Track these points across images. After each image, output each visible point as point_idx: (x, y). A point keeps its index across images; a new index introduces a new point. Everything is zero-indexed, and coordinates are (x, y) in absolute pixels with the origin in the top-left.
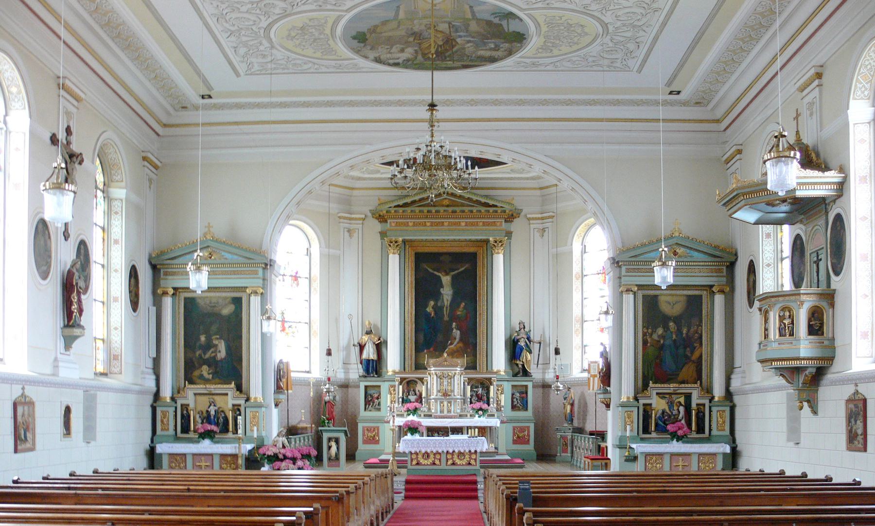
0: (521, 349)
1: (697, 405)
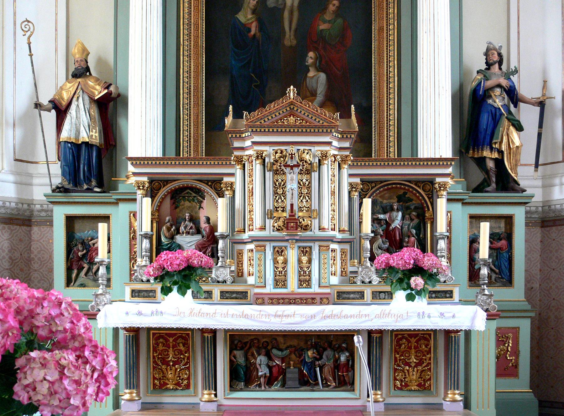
0: (496, 117)
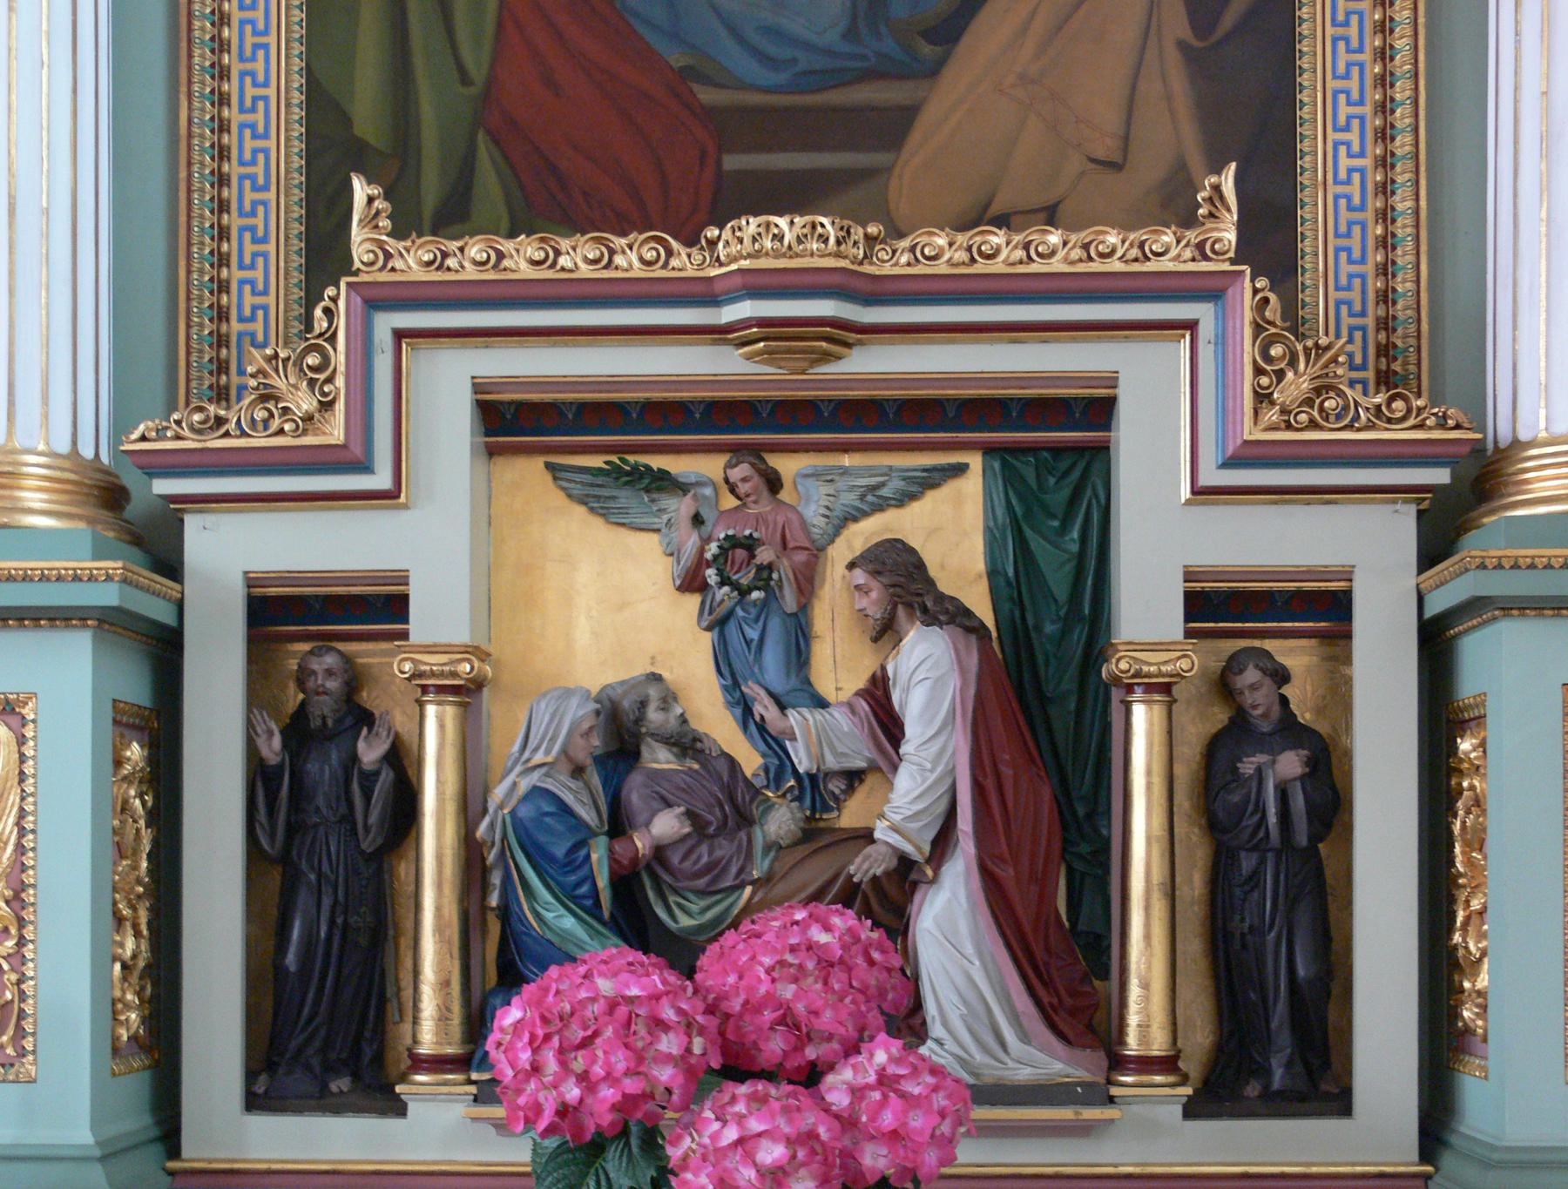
1: (1211, 604)
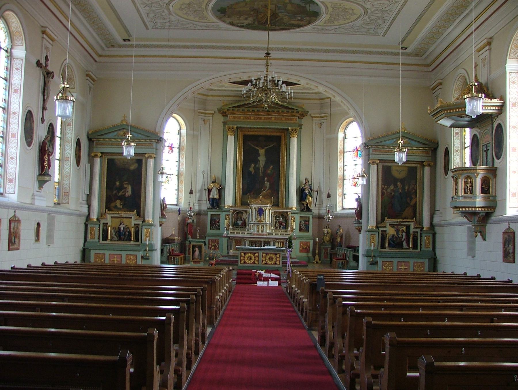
0: (306, 195)
1: (413, 232)
